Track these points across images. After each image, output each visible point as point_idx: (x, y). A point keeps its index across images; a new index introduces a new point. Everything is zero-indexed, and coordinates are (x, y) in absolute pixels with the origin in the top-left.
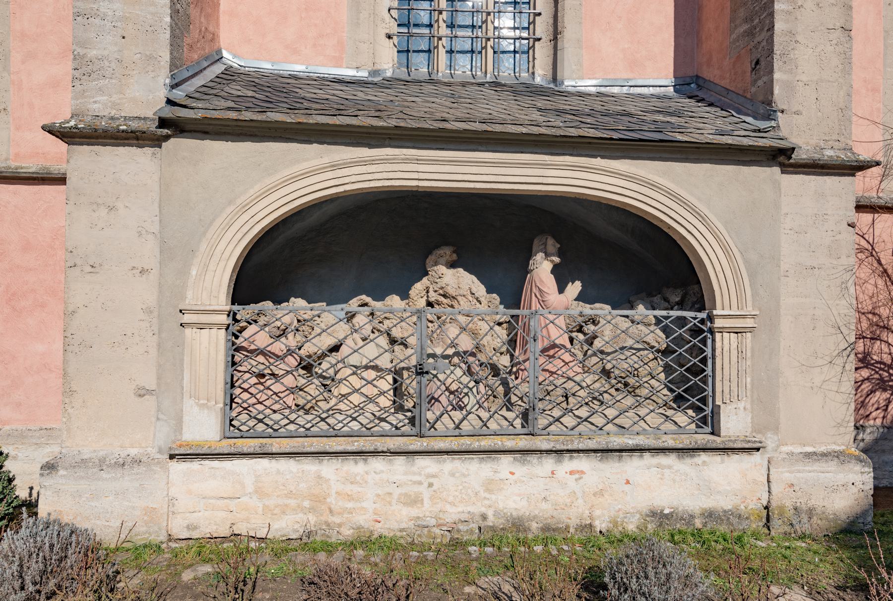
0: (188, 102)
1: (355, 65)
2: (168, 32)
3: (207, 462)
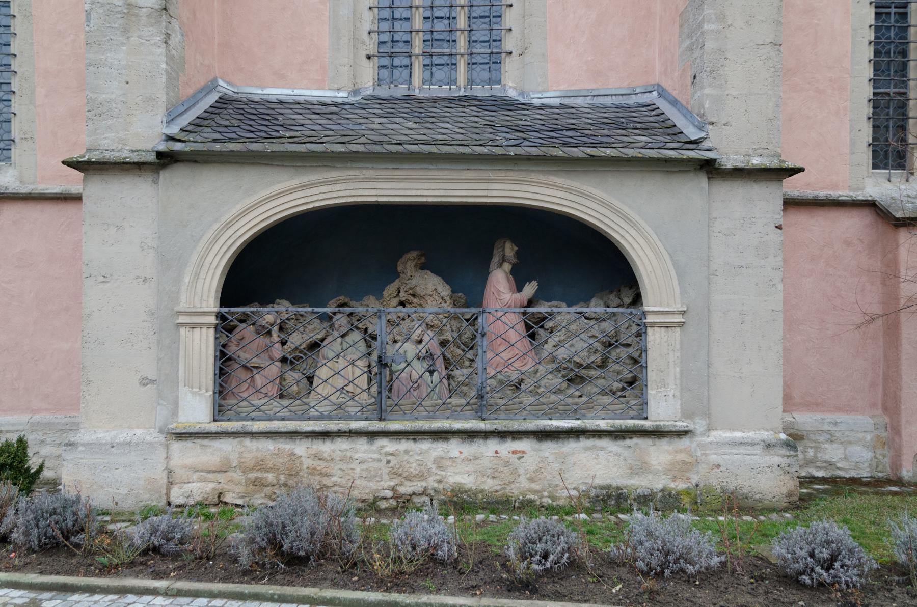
0: (183, 136)
1: (336, 86)
2: (164, 77)
3: (199, 441)
